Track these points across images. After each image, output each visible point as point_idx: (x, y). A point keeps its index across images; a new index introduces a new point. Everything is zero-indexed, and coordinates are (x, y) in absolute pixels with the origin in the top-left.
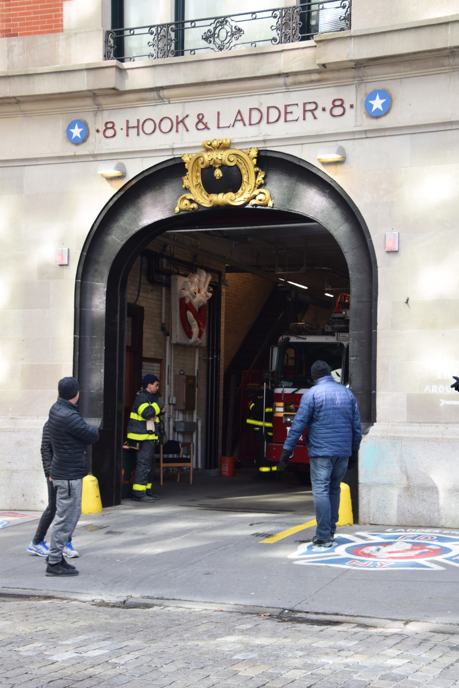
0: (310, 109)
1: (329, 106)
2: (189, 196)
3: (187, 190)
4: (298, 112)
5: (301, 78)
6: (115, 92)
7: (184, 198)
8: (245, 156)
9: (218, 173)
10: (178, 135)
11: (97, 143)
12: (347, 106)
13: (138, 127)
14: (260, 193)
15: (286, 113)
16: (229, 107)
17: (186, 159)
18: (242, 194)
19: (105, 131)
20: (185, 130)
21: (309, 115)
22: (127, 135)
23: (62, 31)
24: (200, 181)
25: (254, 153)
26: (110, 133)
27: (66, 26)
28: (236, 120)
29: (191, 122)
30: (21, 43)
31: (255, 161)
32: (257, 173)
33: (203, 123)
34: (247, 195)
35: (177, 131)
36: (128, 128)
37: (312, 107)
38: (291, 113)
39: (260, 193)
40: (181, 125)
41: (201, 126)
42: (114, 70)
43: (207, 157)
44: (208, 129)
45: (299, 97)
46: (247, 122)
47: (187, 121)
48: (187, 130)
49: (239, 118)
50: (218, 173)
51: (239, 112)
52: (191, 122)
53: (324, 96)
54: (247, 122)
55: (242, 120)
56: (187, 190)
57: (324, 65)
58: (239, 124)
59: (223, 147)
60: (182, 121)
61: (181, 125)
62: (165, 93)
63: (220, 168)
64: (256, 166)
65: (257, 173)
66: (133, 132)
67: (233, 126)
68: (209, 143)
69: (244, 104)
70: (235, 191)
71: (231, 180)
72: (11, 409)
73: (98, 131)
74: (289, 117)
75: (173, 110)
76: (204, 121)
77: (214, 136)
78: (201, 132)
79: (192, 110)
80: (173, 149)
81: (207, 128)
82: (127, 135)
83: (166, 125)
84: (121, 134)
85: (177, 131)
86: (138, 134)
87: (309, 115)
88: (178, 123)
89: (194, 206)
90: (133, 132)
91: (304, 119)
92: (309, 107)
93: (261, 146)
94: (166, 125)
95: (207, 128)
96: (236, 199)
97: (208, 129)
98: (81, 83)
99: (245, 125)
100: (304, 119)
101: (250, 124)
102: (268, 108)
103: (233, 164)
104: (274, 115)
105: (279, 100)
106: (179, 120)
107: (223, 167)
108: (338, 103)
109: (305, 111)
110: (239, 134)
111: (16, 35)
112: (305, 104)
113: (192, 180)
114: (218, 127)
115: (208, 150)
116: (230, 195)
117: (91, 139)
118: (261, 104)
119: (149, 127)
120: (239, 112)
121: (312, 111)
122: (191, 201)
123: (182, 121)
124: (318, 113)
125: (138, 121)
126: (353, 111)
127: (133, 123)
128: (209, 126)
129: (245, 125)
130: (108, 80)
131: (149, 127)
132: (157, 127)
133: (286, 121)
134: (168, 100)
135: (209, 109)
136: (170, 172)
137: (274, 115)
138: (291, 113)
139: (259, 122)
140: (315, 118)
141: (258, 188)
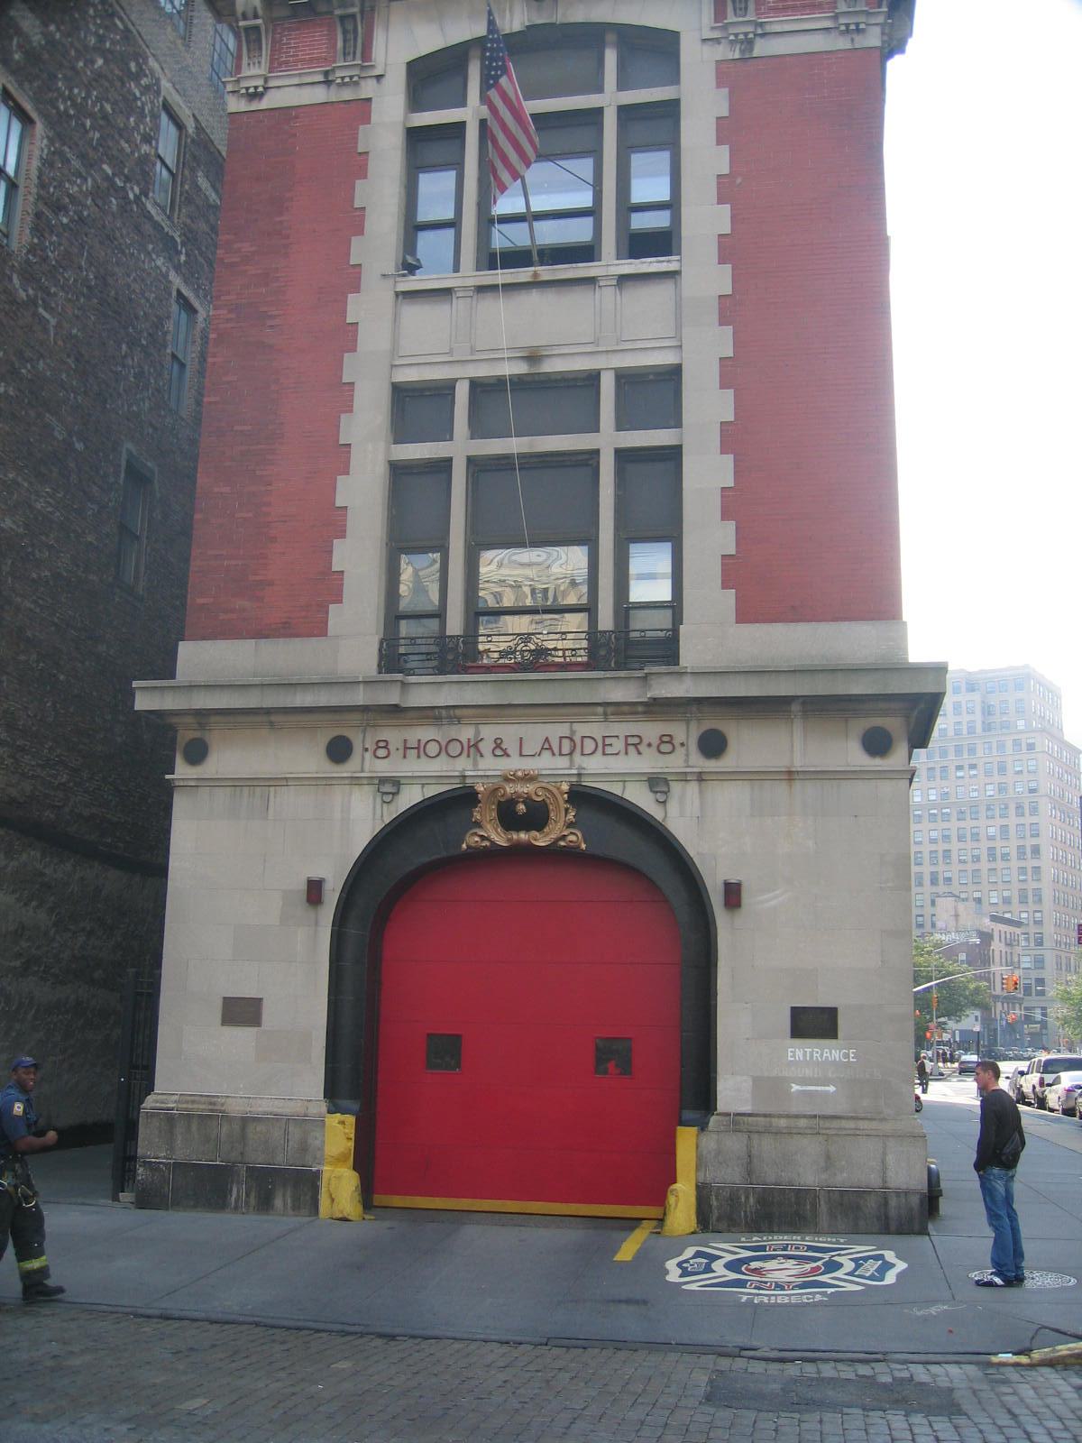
1: (655, 742)
3: (478, 825)
4: (618, 745)
5: (626, 709)
6: (395, 710)
7: (476, 834)
8: (555, 791)
9: (521, 807)
11: (365, 763)
12: (677, 742)
13: (418, 748)
14: (572, 833)
15: (604, 745)
16: (535, 733)
18: (548, 834)
19: (375, 750)
20: (479, 755)
22: (405, 757)
24: (494, 814)
25: (565, 787)
26: (382, 753)
28: (542, 748)
29: (486, 747)
31: (566, 796)
32: (567, 810)
33: (501, 749)
35: (468, 756)
36: (406, 748)
37: (636, 740)
38: (611, 745)
39: (572, 833)
40: (472, 750)
41: (499, 752)
42: (399, 684)
43: (510, 789)
44: (508, 756)
45: (623, 729)
46: (556, 750)
47: (481, 745)
48: (482, 756)
50: (521, 807)
53: (651, 730)
54: (556, 750)
55: (550, 748)
56: (478, 825)
57: (655, 699)
58: (546, 754)
59: (528, 778)
61: (472, 750)
62: (458, 712)
64: (566, 802)
65: (567, 810)
67: (539, 755)
68: (512, 773)
69: (556, 731)
70: (540, 828)
71: (537, 816)
72: (241, 1086)
73: (366, 750)
74: (608, 750)
75: (466, 733)
77: (514, 764)
78: (499, 759)
79: (489, 732)
80: (465, 777)
82: (405, 757)
85: (468, 756)
86: (419, 757)
87: (632, 749)
88: (469, 747)
91: (626, 753)
92: (631, 741)
93: (574, 779)
94: (455, 749)
96: (541, 840)
97: (508, 756)
98: (360, 697)
99: (554, 754)
100: (626, 753)
101: (561, 754)
102: (583, 737)
103: (539, 799)
104: (589, 746)
105: (595, 729)
106: (472, 744)
107: (528, 800)
108: (666, 739)
109: (627, 745)
110: (545, 764)
112: (627, 737)
114: (521, 755)
115: (507, 780)
116: (534, 833)
119: (433, 749)
121: (635, 745)
123: (475, 745)
125: (419, 741)
126: (683, 750)
128: (509, 752)
129: (554, 754)
130: (392, 697)
131: (433, 749)
132: (444, 749)
133: (604, 754)
134: (459, 720)
135: (509, 732)
136: (460, 801)
137: (589, 746)
138: (611, 745)
139: (571, 754)
140: (639, 753)
141: (567, 827)
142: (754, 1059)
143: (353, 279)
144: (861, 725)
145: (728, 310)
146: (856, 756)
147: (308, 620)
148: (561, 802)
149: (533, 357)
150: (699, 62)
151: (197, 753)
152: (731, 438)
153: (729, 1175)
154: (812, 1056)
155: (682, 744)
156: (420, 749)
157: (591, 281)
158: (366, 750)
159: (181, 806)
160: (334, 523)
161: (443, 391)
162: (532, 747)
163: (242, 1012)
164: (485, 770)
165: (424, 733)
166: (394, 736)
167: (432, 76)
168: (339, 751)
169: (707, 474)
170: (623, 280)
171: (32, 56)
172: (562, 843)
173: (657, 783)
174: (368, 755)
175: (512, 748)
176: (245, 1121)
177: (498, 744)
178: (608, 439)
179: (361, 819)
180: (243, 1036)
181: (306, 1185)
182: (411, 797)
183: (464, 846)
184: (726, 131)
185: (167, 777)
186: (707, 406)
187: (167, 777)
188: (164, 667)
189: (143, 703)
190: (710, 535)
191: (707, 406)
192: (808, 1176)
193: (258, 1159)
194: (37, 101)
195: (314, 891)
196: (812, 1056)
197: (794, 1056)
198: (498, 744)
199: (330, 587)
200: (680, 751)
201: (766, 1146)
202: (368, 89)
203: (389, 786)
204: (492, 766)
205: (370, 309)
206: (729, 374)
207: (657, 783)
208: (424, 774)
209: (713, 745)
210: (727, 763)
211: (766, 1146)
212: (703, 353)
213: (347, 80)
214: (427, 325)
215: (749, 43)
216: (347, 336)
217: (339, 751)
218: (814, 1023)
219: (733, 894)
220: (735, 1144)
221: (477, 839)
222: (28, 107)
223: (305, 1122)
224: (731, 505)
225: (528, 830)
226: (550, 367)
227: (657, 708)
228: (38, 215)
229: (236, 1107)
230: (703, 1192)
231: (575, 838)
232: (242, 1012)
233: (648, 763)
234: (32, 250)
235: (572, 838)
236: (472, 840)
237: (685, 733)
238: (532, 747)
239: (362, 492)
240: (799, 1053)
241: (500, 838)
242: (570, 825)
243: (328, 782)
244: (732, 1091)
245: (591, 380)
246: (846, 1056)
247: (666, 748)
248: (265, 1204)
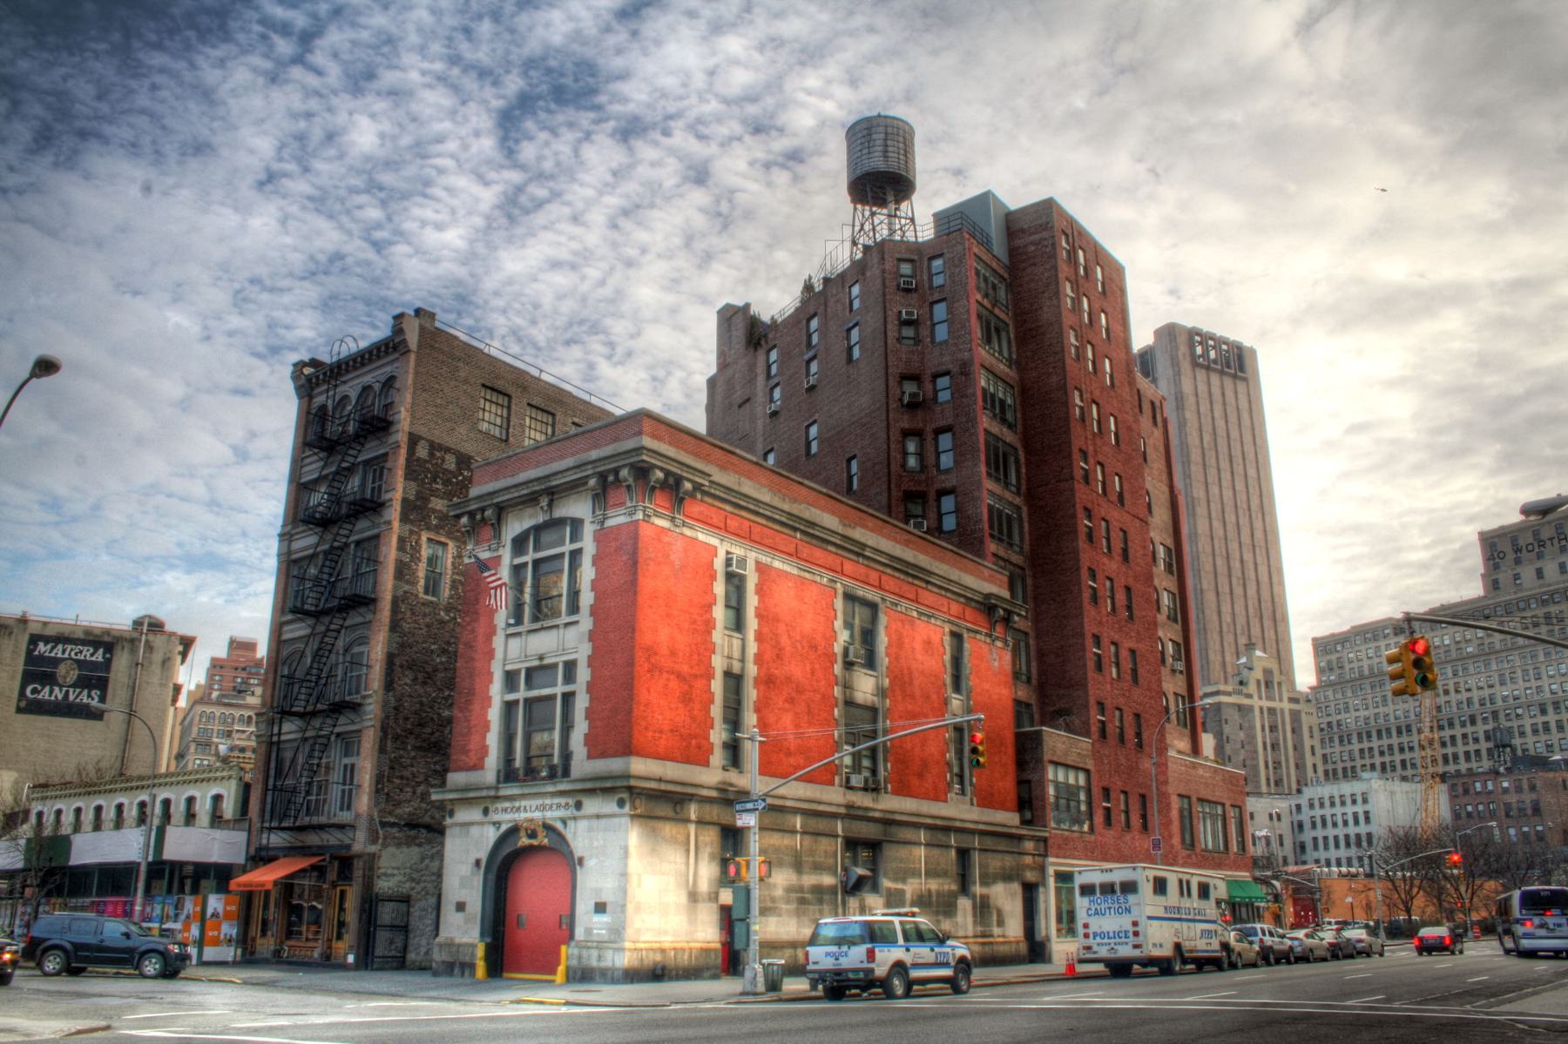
0: (559, 806)
45: (557, 800)
53: (563, 801)
69: (539, 802)
75: (517, 804)
77: (529, 815)
79: (523, 803)
96: (535, 842)
105: (548, 801)
110: (537, 815)
113: (523, 833)
142: (588, 923)
143: (492, 631)
144: (617, 797)
146: (616, 809)
147: (478, 766)
149: (541, 658)
150: (589, 530)
151: (451, 814)
152: (591, 688)
153: (574, 963)
156: (505, 810)
157: (557, 626)
159: (448, 832)
160: (486, 727)
161: (518, 672)
163: (461, 907)
165: (507, 804)
166: (500, 805)
167: (519, 544)
168: (486, 812)
169: (582, 703)
170: (567, 625)
171: (443, 518)
173: (564, 821)
176: (459, 945)
178: (559, 689)
179: (491, 835)
180: (460, 915)
181: (472, 966)
182: (504, 828)
184: (596, 561)
186: (583, 674)
188: (443, 783)
189: (434, 797)
190: (581, 727)
191: (583, 674)
192: (594, 963)
193: (461, 958)
194: (449, 535)
195: (478, 863)
199: (484, 750)
201: (584, 952)
202: (501, 552)
203: (497, 824)
204: (523, 815)
205: (498, 641)
206: (591, 661)
207: (564, 821)
208: (506, 817)
209: (578, 805)
210: (583, 812)
211: (584, 952)
212: (582, 652)
214: (515, 644)
215: (602, 523)
216: (490, 654)
217: (486, 812)
218: (600, 908)
219: (581, 861)
220: (576, 951)
222: (443, 539)
223: (474, 946)
226: (546, 661)
227: (562, 793)
228: (454, 581)
229: (457, 941)
230: (568, 968)
231: (546, 841)
232: (461, 907)
233: (561, 813)
234: (451, 597)
236: (520, 844)
237: (571, 801)
239: (494, 714)
243: (482, 824)
244: (579, 933)
245: (555, 666)
248: (463, 974)
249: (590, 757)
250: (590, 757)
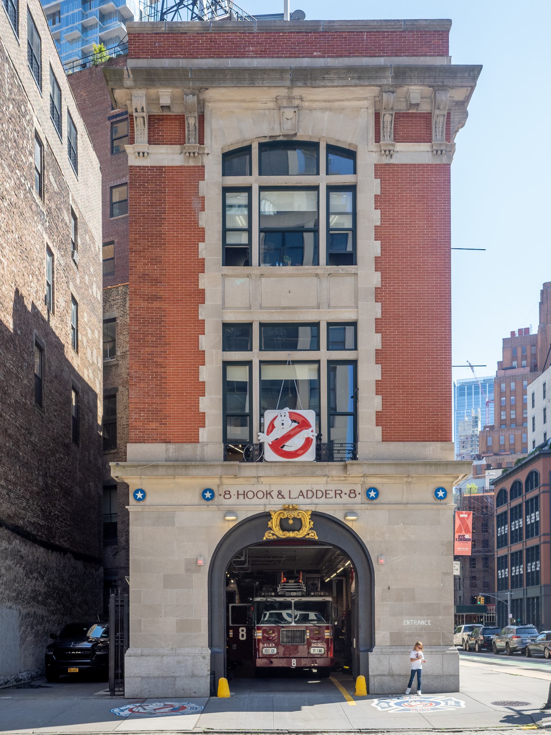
2: (272, 532)
3: (271, 529)
4: (332, 494)
9: (291, 522)
10: (267, 500)
12: (357, 493)
13: (244, 494)
17: (273, 514)
21: (338, 496)
23: (198, 442)
25: (310, 513)
26: (227, 496)
27: (200, 440)
29: (275, 494)
30: (174, 447)
34: (305, 533)
36: (238, 494)
37: (340, 492)
40: (268, 495)
41: (280, 496)
43: (286, 514)
47: (271, 493)
49: (301, 494)
50: (291, 522)
51: (301, 491)
52: (275, 494)
55: (303, 495)
58: (301, 497)
60: (270, 493)
61: (268, 495)
63: (292, 519)
66: (241, 497)
71: (298, 524)
76: (282, 494)
81: (283, 497)
83: (260, 495)
84: (234, 498)
87: (338, 496)
88: (267, 494)
89: (275, 537)
90: (241, 497)
92: (337, 492)
94: (260, 495)
95: (283, 497)
103: (299, 517)
104: (320, 494)
106: (268, 492)
107: (294, 519)
109: (336, 494)
111: (170, 442)
113: (274, 523)
117: (216, 499)
118: (313, 488)
119: (250, 495)
120: (301, 491)
121: (340, 494)
122: (273, 534)
123: (270, 493)
124: (342, 495)
126: (360, 496)
127: (241, 492)
131: (250, 495)
132: (255, 495)
145: (379, 294)
148: (308, 519)
154: (413, 623)
155: (359, 494)
158: (220, 495)
162: (294, 494)
164: (274, 505)
172: (308, 537)
174: (222, 497)
175: (286, 495)
177: (280, 493)
183: (265, 539)
185: (126, 507)
186: (370, 341)
187: (126, 507)
191: (370, 341)
196: (413, 623)
197: (406, 623)
198: (280, 493)
200: (359, 498)
206: (380, 326)
213: (192, 155)
221: (271, 535)
224: (380, 388)
225: (293, 530)
235: (313, 534)
236: (268, 536)
238: (294, 494)
240: (408, 622)
241: (281, 534)
242: (311, 529)
246: (427, 623)
247: (352, 495)
249: (386, 439)
250: (386, 439)
